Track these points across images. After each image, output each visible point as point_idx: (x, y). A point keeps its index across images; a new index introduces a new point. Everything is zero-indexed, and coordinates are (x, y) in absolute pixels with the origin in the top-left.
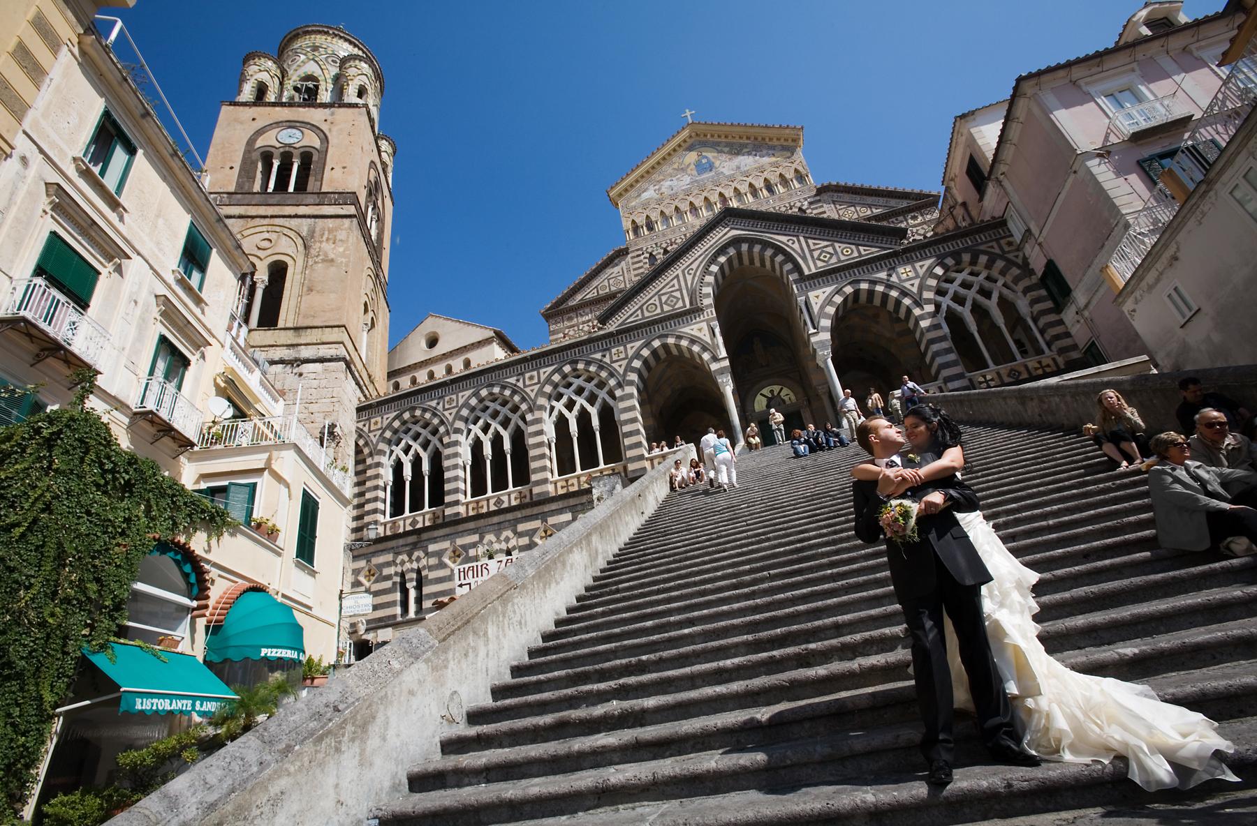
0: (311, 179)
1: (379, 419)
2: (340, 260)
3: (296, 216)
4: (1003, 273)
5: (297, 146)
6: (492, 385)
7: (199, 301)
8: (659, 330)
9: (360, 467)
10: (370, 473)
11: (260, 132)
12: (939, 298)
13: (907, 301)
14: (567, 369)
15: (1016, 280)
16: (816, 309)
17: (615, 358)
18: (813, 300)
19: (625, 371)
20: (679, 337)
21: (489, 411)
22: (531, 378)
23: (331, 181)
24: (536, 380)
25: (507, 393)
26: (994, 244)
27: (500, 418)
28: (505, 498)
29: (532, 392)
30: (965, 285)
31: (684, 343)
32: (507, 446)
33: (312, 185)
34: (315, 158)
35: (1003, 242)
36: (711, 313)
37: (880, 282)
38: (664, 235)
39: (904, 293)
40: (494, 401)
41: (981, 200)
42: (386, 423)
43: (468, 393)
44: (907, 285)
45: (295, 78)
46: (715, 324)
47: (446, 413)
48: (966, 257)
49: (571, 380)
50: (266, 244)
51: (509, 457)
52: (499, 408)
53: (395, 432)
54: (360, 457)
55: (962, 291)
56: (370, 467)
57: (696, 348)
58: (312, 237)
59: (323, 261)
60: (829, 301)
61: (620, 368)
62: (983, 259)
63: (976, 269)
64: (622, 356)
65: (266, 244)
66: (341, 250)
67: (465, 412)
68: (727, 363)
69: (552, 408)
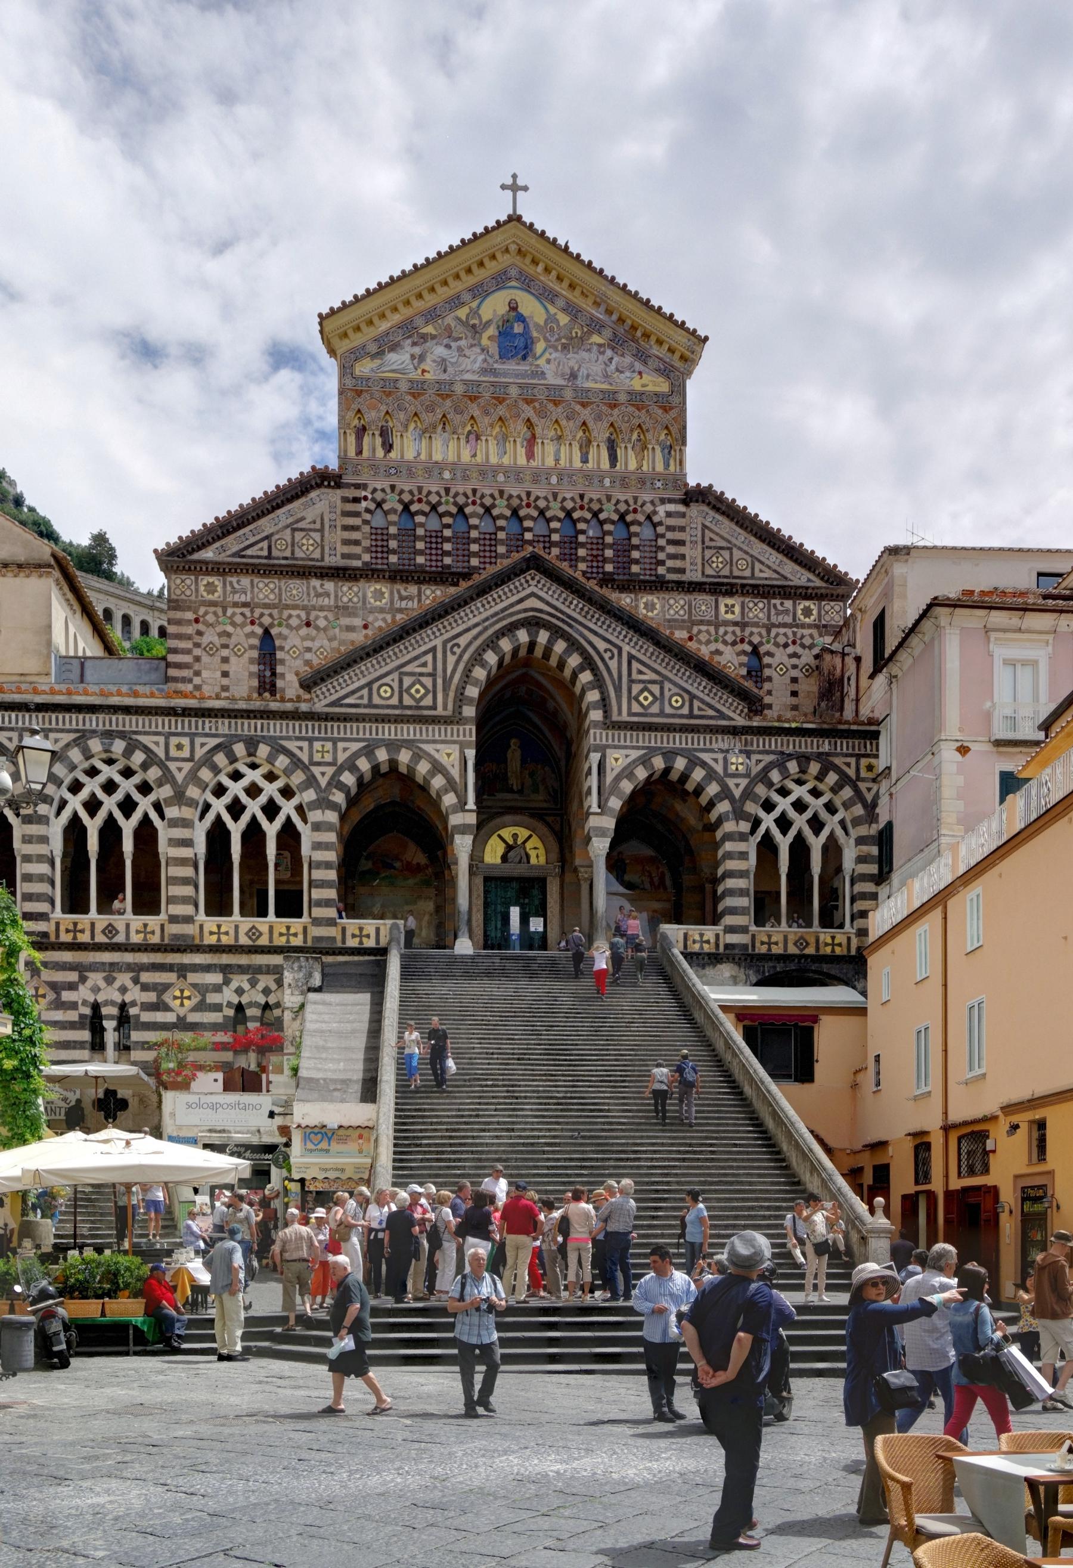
4: (847, 805)
6: (109, 735)
8: (388, 731)
12: (762, 814)
13: (723, 807)
14: (239, 749)
15: (857, 822)
16: (609, 778)
17: (317, 757)
18: (610, 762)
19: (329, 784)
20: (417, 757)
22: (179, 747)
24: (186, 753)
25: (138, 757)
26: (853, 761)
29: (180, 771)
30: (800, 806)
31: (423, 768)
35: (864, 762)
36: (469, 733)
37: (704, 764)
38: (411, 474)
39: (725, 793)
40: (110, 762)
41: (872, 677)
44: (731, 782)
46: (471, 754)
48: (814, 768)
49: (244, 769)
55: (792, 814)
57: (438, 782)
60: (627, 773)
61: (323, 775)
62: (832, 778)
63: (821, 787)
64: (328, 758)
68: (472, 819)
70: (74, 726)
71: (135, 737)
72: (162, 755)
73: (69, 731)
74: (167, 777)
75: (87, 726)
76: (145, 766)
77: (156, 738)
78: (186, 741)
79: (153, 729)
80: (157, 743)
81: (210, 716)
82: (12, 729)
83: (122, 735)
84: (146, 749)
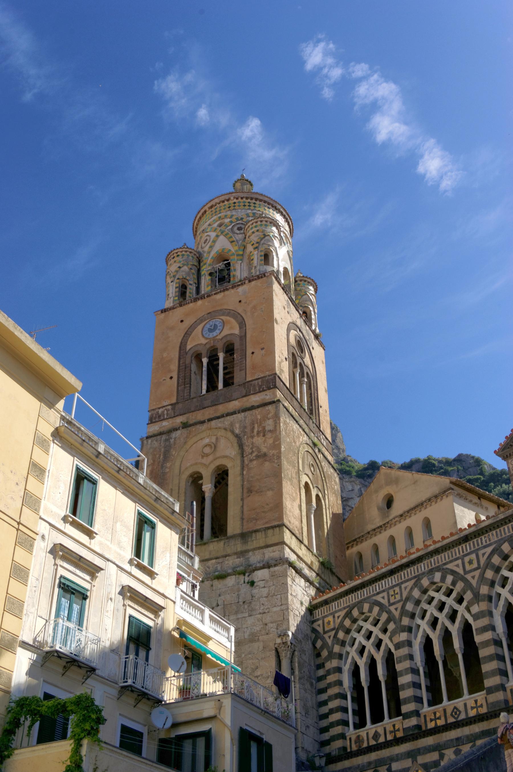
0: (236, 369)
1: (330, 618)
2: (272, 452)
3: (228, 415)
5: (220, 337)
6: (431, 572)
7: (152, 574)
9: (321, 672)
10: (331, 678)
11: (187, 334)
21: (435, 602)
22: (471, 562)
23: (254, 367)
24: (475, 565)
27: (446, 610)
28: (461, 708)
32: (457, 644)
33: (238, 378)
34: (237, 346)
42: (338, 621)
43: (410, 584)
45: (209, 261)
47: (392, 608)
50: (207, 450)
51: (460, 657)
52: (444, 598)
53: (348, 631)
54: (319, 661)
56: (328, 673)
58: (245, 433)
59: (258, 457)
65: (207, 450)
66: (271, 441)
67: (410, 607)
69: (499, 595)
70: (413, 575)
71: (445, 567)
72: (461, 572)
73: (410, 579)
74: (468, 585)
75: (420, 572)
76: (454, 583)
77: (456, 563)
78: (473, 556)
79: (454, 557)
80: (457, 566)
81: (483, 534)
82: (384, 591)
83: (438, 569)
84: (453, 573)
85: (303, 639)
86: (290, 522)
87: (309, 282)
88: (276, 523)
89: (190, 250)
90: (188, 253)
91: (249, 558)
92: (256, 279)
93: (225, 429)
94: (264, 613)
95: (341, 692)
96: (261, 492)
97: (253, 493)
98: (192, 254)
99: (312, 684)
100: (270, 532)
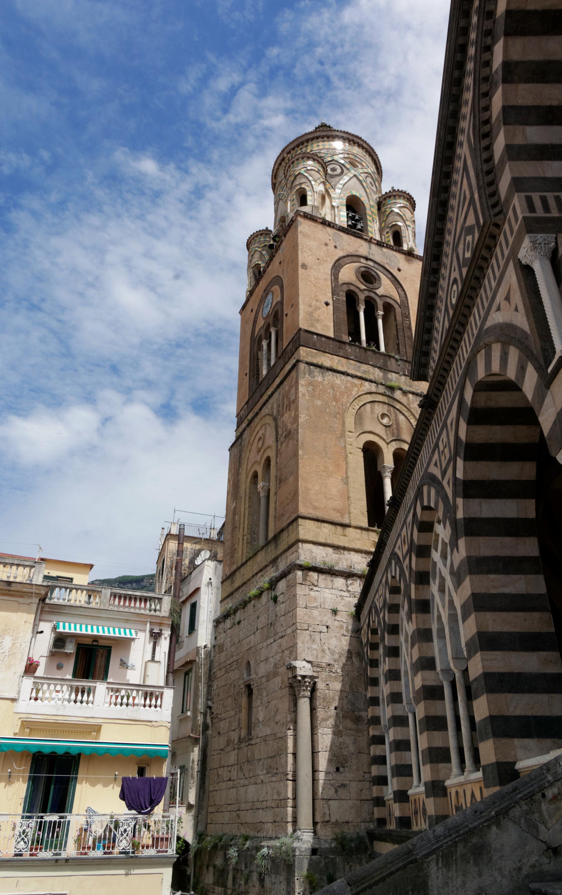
11: (255, 322)
59: (286, 437)
85: (335, 661)
86: (315, 508)
87: (395, 196)
88: (295, 516)
89: (260, 233)
90: (259, 236)
91: (278, 566)
92: (288, 230)
93: (269, 415)
94: (283, 637)
95: (377, 733)
96: (287, 479)
97: (283, 482)
98: (264, 235)
99: (357, 720)
100: (291, 527)
